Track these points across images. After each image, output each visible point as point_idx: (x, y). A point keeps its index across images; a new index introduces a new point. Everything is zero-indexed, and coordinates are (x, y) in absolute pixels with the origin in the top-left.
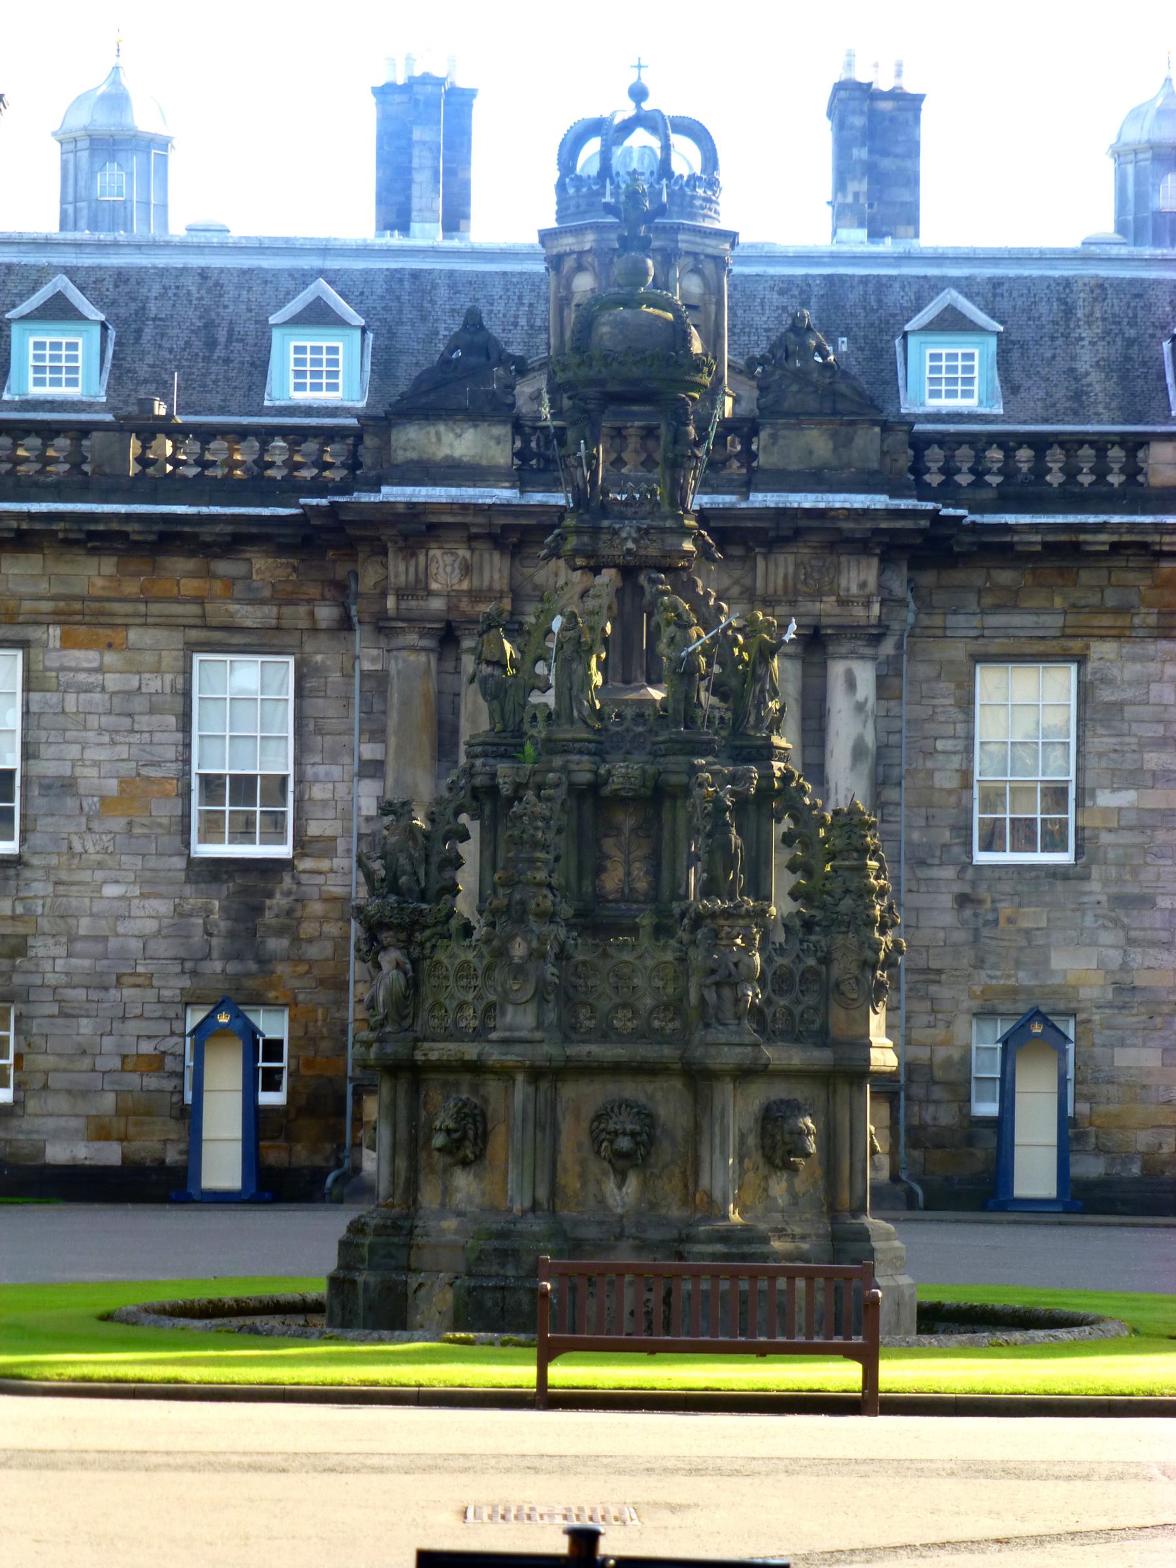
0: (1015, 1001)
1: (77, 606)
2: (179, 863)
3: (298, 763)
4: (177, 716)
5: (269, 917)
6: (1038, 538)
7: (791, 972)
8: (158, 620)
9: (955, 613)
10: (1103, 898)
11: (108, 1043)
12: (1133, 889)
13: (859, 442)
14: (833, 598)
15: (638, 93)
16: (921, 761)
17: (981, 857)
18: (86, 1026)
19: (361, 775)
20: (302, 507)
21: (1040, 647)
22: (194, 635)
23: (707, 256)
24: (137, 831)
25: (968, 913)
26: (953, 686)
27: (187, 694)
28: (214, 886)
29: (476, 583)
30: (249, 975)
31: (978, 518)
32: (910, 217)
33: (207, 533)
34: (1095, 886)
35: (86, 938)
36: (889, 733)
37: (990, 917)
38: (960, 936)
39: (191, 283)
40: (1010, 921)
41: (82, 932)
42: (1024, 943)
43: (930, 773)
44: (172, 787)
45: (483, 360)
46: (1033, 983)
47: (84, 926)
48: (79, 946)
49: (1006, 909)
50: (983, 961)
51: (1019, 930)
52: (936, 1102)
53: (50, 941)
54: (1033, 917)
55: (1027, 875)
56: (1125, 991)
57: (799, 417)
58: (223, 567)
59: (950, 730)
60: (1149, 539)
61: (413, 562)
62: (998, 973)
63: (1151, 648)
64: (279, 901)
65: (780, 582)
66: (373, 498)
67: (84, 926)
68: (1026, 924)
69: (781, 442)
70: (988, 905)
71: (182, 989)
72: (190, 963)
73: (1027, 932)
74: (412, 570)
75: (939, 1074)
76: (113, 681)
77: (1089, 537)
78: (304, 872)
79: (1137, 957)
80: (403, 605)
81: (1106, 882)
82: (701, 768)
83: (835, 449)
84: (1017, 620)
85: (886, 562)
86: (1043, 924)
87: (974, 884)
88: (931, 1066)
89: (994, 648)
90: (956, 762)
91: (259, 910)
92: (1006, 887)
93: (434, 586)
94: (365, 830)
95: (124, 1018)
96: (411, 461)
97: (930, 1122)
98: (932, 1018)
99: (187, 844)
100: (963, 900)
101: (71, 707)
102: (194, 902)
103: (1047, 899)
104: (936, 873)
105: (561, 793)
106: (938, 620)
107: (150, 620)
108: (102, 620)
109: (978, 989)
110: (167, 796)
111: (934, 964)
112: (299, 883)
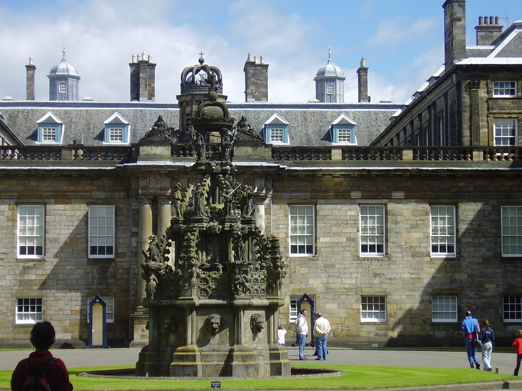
1: (59, 194)
2: (86, 260)
3: (116, 233)
5: (109, 274)
7: (257, 280)
10: (322, 265)
11: (68, 307)
12: (330, 263)
15: (201, 61)
18: (62, 303)
19: (132, 236)
20: (117, 167)
22: (89, 200)
24: (74, 252)
29: (162, 186)
30: (104, 289)
31: (289, 168)
34: (320, 262)
35: (61, 280)
37: (294, 270)
39: (84, 114)
41: (60, 278)
44: (83, 240)
45: (163, 128)
47: (61, 277)
48: (60, 282)
49: (298, 268)
51: (301, 274)
53: (52, 281)
54: (304, 270)
56: (328, 289)
58: (96, 183)
59: (282, 222)
60: (332, 173)
63: (333, 201)
64: (111, 269)
66: (135, 164)
67: (61, 277)
68: (303, 272)
73: (303, 274)
76: (68, 213)
77: (317, 173)
79: (331, 280)
80: (143, 192)
81: (323, 261)
82: (234, 226)
85: (266, 179)
86: (307, 272)
89: (293, 201)
90: (285, 231)
91: (106, 272)
93: (151, 186)
94: (133, 250)
95: (71, 301)
101: (57, 220)
102: (88, 270)
103: (308, 265)
105: (197, 233)
106: (279, 194)
108: (65, 197)
109: (291, 289)
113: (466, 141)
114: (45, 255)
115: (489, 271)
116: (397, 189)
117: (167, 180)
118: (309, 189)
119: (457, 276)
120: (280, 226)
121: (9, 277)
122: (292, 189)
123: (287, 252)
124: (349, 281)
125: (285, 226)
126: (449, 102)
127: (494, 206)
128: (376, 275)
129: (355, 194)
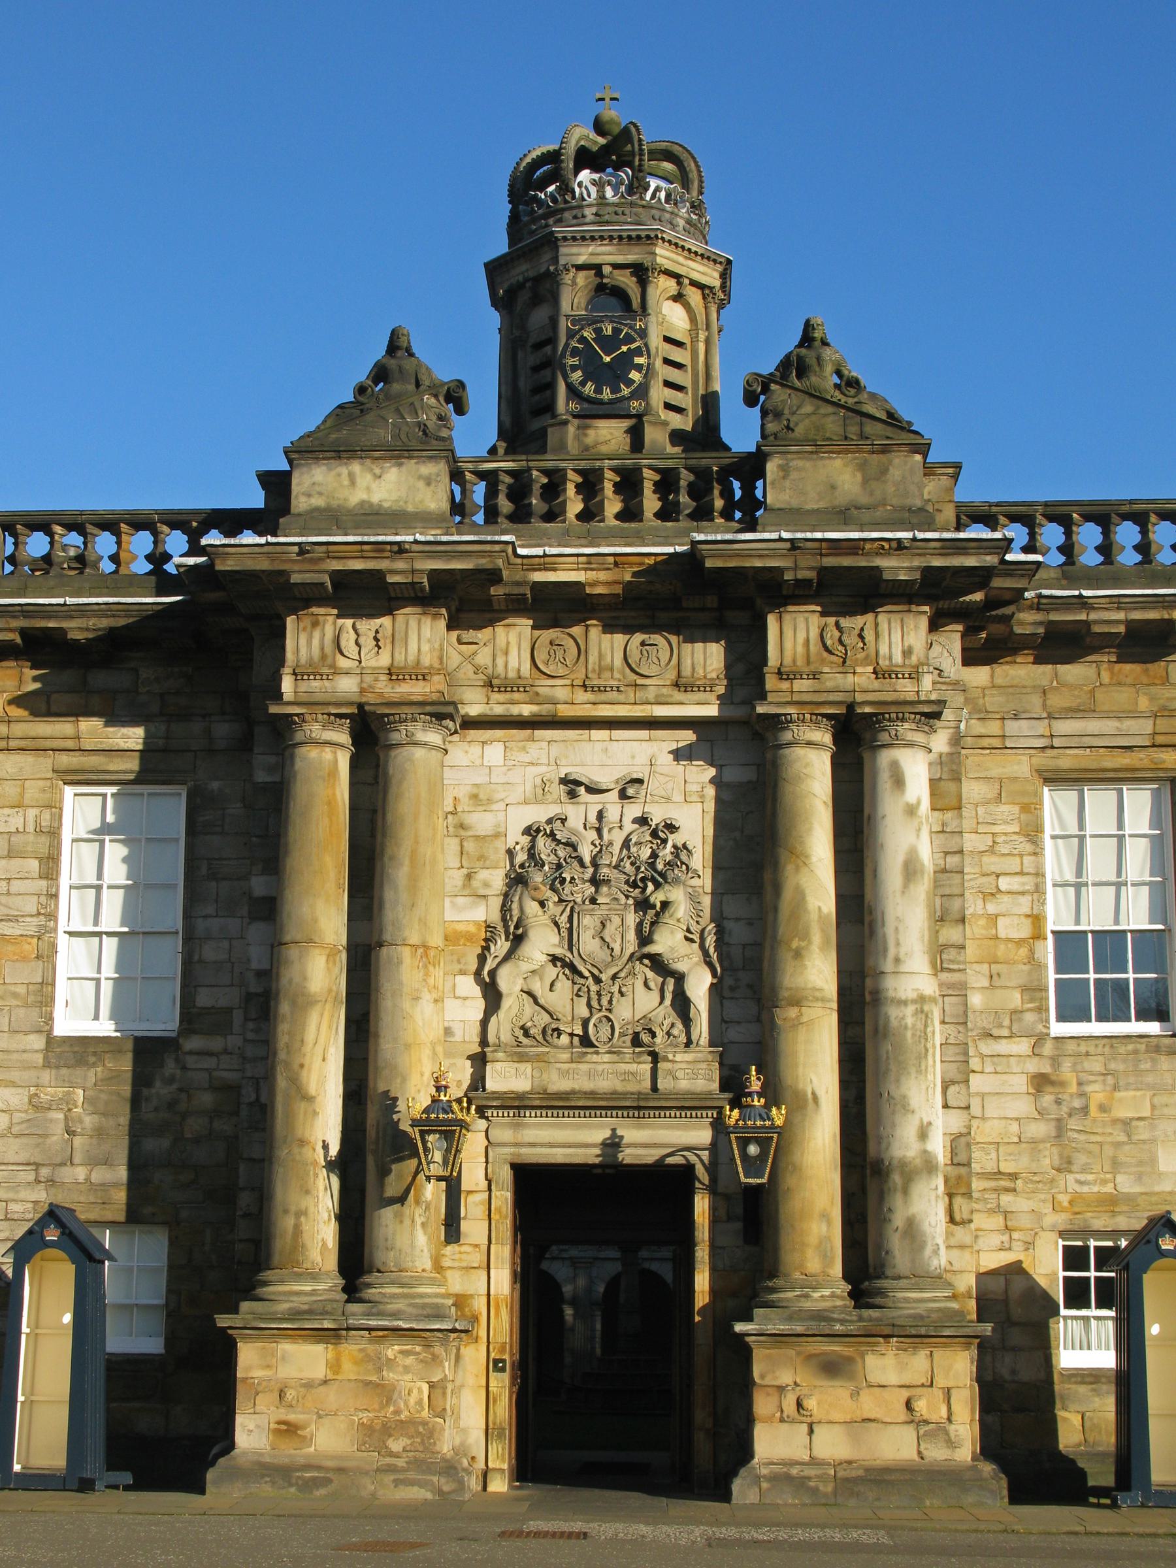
0: (1114, 1214)
2: (38, 1042)
4: (40, 860)
6: (1121, 616)
8: (22, 744)
9: (1016, 717)
13: (895, 473)
14: (870, 669)
16: (980, 903)
17: (1059, 1029)
19: (254, 917)
21: (1125, 760)
22: (65, 760)
23: (694, 283)
25: (1047, 1100)
26: (1016, 809)
27: (54, 833)
28: (79, 1072)
33: (77, 630)
36: (946, 853)
37: (1077, 1103)
38: (1039, 1129)
40: (1103, 1108)
42: (1122, 1138)
43: (993, 919)
46: (1137, 1189)
49: (1097, 1092)
50: (1069, 1163)
51: (1115, 1121)
52: (1013, 1349)
54: (1131, 1104)
55: (1122, 1049)
57: (818, 445)
59: (1013, 864)
61: (317, 634)
62: (1090, 1177)
65: (800, 649)
69: (794, 475)
70: (1073, 1088)
71: (35, 1202)
73: (1126, 1124)
74: (316, 642)
75: (1017, 1312)
78: (191, 1053)
80: (303, 686)
83: (865, 481)
84: (1093, 726)
87: (1055, 1061)
88: (1006, 1301)
89: (1066, 761)
90: (1024, 905)
92: (1096, 1065)
96: (317, 509)
97: (1007, 1377)
98: (1006, 1238)
99: (50, 1019)
100: (1041, 1082)
102: (50, 1093)
103: (1150, 1079)
104: (1003, 1047)
106: (993, 727)
107: (13, 744)
109: (1064, 1199)
110: (24, 959)
111: (1006, 1167)
112: (184, 1068)
117: (426, 631)
118: (1144, 703)
120: (1004, 883)
122: (1055, 701)
123: (1042, 1009)
125: (1028, 883)
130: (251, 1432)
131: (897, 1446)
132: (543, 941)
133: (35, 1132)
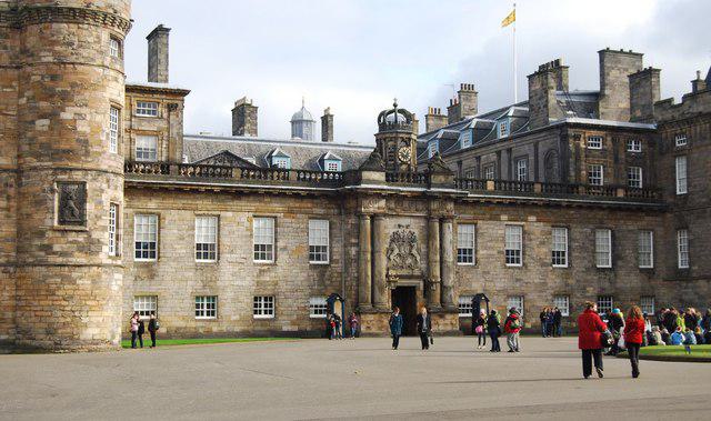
15: (395, 105)
32: (256, 133)
57: (438, 173)
64: (328, 273)
72: (311, 287)
102: (311, 273)
113: (572, 180)
114: (276, 259)
115: (589, 277)
116: (532, 214)
119: (570, 281)
121: (248, 278)
124: (499, 285)
126: (542, 149)
127: (592, 229)
128: (517, 280)
129: (504, 217)
130: (363, 329)
131: (449, 328)
132: (396, 251)
133: (308, 279)
